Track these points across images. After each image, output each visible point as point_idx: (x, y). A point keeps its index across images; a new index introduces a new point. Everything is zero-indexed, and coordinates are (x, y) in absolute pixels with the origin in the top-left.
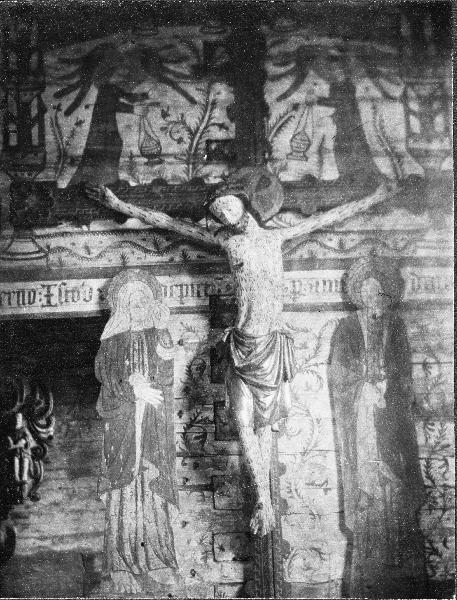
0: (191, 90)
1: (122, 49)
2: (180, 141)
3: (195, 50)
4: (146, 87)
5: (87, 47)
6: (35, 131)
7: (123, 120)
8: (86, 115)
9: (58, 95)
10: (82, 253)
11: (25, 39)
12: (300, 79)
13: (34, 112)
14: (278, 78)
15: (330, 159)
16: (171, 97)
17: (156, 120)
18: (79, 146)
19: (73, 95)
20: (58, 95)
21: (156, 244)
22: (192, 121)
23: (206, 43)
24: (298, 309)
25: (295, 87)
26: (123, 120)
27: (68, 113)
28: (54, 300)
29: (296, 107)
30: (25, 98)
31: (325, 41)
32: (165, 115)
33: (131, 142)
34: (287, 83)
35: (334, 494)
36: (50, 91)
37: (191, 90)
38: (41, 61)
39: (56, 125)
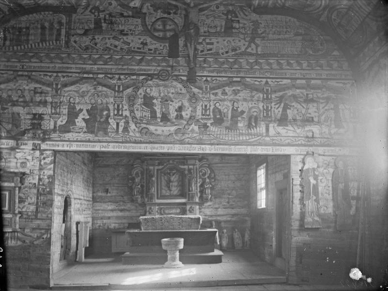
0: (303, 105)
1: (289, 94)
2: (301, 117)
3: (304, 95)
4: (293, 104)
5: (281, 93)
6: (270, 113)
7: (288, 111)
8: (280, 109)
9: (275, 105)
10: (280, 141)
11: (267, 90)
12: (327, 103)
13: (270, 108)
14: (322, 103)
15: (333, 122)
16: (299, 106)
17: (296, 112)
18: (279, 116)
19: (277, 106)
20: (275, 105)
21: (295, 140)
22: (303, 112)
23: (307, 94)
24: (326, 155)
25: (327, 105)
26: (288, 111)
27: (277, 109)
28: (274, 151)
29: (326, 110)
30: (268, 105)
31: (333, 95)
32: (298, 110)
33: (290, 117)
34: (323, 105)
35: (331, 196)
36: (273, 104)
37: (303, 105)
38: (271, 97)
39: (274, 111)
